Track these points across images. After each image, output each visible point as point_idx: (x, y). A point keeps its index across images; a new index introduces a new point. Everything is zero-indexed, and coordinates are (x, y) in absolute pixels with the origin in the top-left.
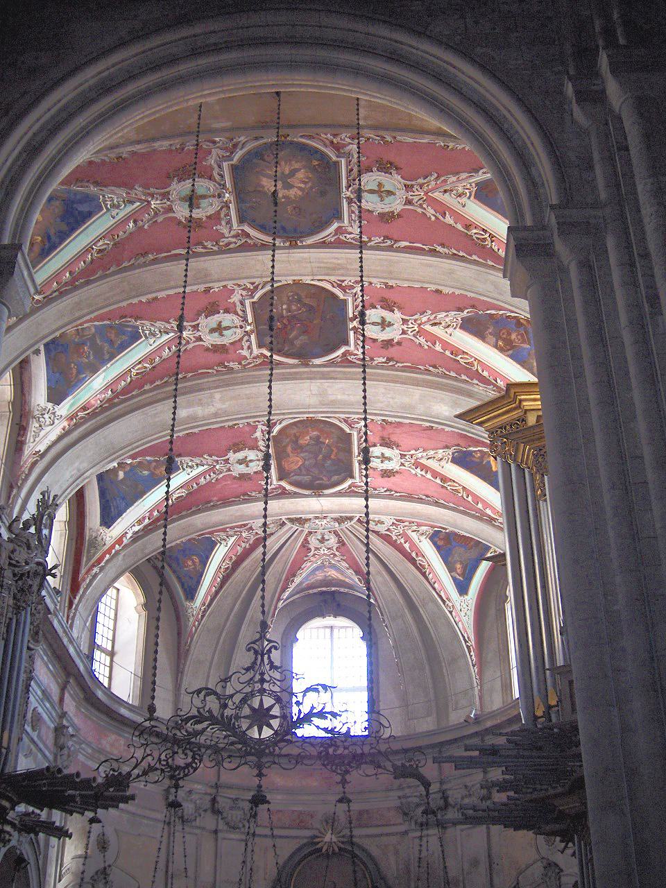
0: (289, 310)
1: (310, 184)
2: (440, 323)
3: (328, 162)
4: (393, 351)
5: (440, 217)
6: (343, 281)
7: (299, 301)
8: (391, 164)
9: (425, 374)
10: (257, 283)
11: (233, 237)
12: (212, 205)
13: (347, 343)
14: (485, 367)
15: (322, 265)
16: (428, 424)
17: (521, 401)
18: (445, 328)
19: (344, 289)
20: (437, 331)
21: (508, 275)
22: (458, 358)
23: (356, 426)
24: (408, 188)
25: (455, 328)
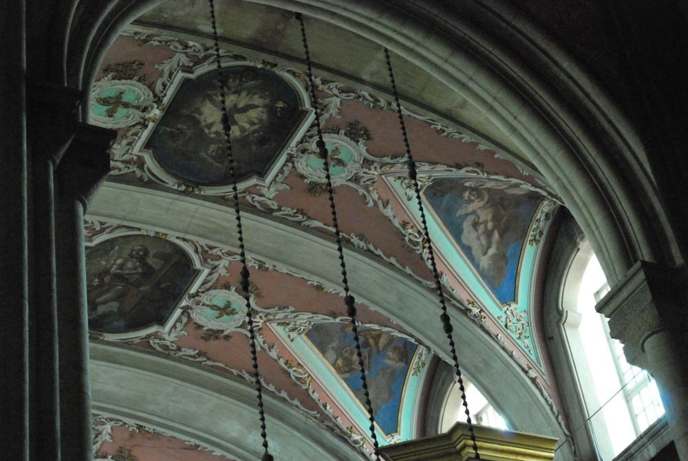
0: (121, 267)
1: (256, 127)
2: (288, 324)
3: (296, 108)
4: (213, 346)
5: (381, 205)
6: (212, 248)
7: (142, 259)
8: (366, 131)
9: (235, 380)
10: (105, 226)
11: (123, 162)
12: (127, 117)
13: (162, 321)
14: (319, 388)
15: (201, 223)
16: (194, 441)
17: (465, 446)
18: (290, 331)
19: (206, 255)
20: (281, 332)
21: (608, 310)
22: (290, 371)
23: (100, 428)
24: (367, 163)
25: (300, 334)
